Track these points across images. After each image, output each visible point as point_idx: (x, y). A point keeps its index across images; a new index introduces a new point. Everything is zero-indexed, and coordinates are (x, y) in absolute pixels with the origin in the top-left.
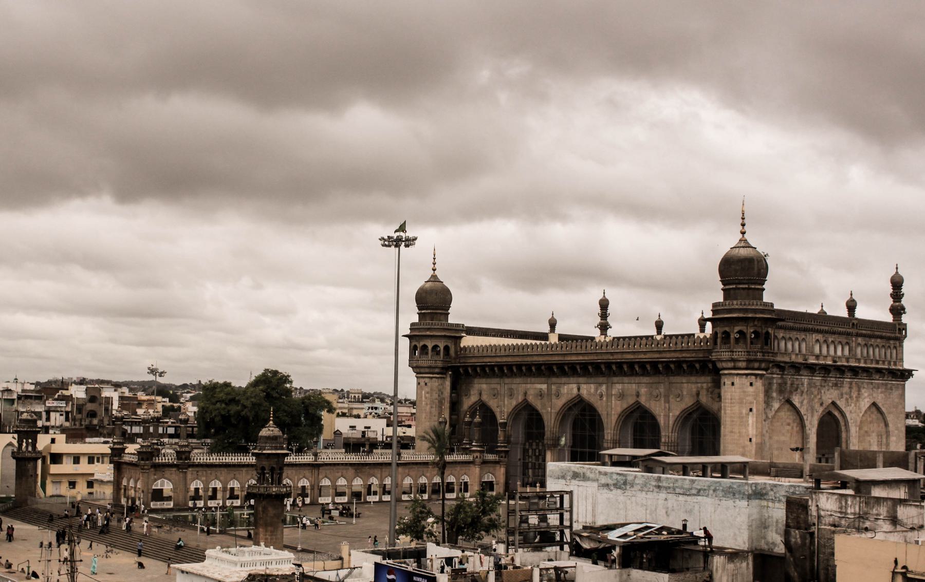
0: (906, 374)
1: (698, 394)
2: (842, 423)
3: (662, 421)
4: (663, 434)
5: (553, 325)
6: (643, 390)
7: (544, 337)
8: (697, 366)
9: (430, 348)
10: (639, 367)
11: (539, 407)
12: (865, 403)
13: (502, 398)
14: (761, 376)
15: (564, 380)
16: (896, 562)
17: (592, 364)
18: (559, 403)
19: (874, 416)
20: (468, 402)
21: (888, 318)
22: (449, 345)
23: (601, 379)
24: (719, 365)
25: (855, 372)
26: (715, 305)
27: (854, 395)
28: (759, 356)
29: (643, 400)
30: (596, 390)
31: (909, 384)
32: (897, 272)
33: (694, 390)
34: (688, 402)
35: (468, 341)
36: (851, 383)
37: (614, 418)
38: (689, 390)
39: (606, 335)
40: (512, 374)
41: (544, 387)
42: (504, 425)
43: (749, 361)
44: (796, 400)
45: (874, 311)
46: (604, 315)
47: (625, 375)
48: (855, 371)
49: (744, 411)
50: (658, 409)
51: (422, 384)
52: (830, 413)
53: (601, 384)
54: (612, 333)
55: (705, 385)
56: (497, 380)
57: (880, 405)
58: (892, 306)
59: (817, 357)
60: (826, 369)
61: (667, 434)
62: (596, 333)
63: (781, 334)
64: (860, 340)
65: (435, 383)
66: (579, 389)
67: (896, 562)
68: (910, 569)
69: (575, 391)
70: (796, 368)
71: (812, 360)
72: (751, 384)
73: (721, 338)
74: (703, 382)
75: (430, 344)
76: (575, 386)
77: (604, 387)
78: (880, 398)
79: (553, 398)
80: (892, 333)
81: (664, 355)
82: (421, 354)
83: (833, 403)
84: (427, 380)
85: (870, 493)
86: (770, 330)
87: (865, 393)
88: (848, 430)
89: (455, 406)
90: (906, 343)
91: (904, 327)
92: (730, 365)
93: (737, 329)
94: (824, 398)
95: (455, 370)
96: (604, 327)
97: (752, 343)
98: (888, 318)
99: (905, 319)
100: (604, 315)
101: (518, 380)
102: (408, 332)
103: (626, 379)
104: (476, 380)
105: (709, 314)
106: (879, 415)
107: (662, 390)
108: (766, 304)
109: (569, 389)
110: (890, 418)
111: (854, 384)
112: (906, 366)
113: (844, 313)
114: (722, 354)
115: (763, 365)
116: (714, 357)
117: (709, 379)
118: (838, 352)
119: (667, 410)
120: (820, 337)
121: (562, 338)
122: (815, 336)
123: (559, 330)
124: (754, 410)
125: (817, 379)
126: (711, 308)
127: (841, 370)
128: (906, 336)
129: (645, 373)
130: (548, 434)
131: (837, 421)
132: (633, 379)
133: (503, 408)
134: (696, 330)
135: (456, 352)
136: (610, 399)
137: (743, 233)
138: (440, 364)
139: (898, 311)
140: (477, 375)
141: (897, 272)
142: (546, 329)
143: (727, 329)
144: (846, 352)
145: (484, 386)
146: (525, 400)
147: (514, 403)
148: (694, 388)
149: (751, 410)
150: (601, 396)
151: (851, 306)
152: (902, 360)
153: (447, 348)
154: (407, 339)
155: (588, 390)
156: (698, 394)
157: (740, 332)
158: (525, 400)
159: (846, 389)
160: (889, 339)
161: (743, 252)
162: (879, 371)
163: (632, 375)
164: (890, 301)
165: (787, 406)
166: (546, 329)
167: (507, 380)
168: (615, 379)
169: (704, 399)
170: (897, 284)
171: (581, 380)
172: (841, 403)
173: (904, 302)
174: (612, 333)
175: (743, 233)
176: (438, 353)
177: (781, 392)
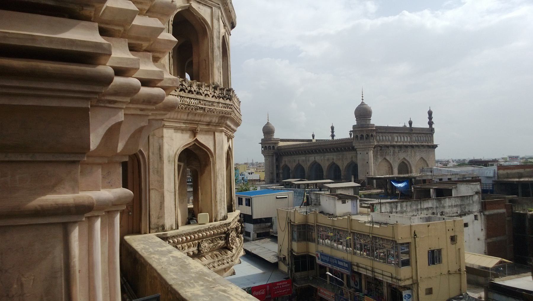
0: (435, 146)
4: (342, 172)
5: (313, 136)
6: (335, 158)
7: (311, 140)
12: (418, 158)
18: (309, 164)
24: (356, 147)
26: (354, 126)
29: (335, 161)
31: (436, 149)
34: (349, 161)
35: (281, 144)
37: (326, 168)
38: (348, 156)
40: (294, 154)
44: (388, 158)
45: (421, 123)
46: (333, 132)
47: (328, 152)
48: (412, 146)
50: (339, 164)
52: (403, 162)
54: (335, 138)
57: (424, 158)
59: (396, 142)
60: (400, 147)
62: (330, 138)
63: (381, 135)
64: (414, 135)
70: (387, 146)
71: (395, 143)
74: (352, 154)
75: (267, 146)
80: (430, 132)
82: (264, 149)
85: (336, 192)
87: (418, 154)
88: (411, 168)
89: (278, 167)
90: (435, 135)
95: (276, 154)
96: (333, 136)
97: (366, 139)
98: (428, 126)
99: (433, 126)
100: (333, 132)
103: (329, 154)
105: (352, 130)
108: (371, 125)
109: (312, 158)
110: (428, 162)
112: (435, 143)
113: (408, 126)
114: (356, 145)
118: (406, 140)
119: (343, 165)
120: (397, 135)
121: (316, 140)
122: (395, 135)
123: (316, 138)
125: (397, 150)
127: (406, 146)
129: (335, 152)
130: (306, 175)
131: (406, 165)
132: (331, 154)
133: (292, 166)
137: (363, 100)
139: (431, 123)
142: (312, 138)
146: (299, 163)
147: (295, 164)
151: (410, 123)
152: (433, 141)
153: (273, 147)
158: (299, 163)
159: (409, 153)
160: (428, 134)
162: (423, 146)
164: (428, 120)
165: (385, 160)
166: (312, 138)
167: (293, 157)
168: (326, 154)
169: (354, 159)
170: (430, 113)
172: (407, 158)
173: (433, 120)
174: (335, 138)
175: (363, 100)
177: (381, 155)
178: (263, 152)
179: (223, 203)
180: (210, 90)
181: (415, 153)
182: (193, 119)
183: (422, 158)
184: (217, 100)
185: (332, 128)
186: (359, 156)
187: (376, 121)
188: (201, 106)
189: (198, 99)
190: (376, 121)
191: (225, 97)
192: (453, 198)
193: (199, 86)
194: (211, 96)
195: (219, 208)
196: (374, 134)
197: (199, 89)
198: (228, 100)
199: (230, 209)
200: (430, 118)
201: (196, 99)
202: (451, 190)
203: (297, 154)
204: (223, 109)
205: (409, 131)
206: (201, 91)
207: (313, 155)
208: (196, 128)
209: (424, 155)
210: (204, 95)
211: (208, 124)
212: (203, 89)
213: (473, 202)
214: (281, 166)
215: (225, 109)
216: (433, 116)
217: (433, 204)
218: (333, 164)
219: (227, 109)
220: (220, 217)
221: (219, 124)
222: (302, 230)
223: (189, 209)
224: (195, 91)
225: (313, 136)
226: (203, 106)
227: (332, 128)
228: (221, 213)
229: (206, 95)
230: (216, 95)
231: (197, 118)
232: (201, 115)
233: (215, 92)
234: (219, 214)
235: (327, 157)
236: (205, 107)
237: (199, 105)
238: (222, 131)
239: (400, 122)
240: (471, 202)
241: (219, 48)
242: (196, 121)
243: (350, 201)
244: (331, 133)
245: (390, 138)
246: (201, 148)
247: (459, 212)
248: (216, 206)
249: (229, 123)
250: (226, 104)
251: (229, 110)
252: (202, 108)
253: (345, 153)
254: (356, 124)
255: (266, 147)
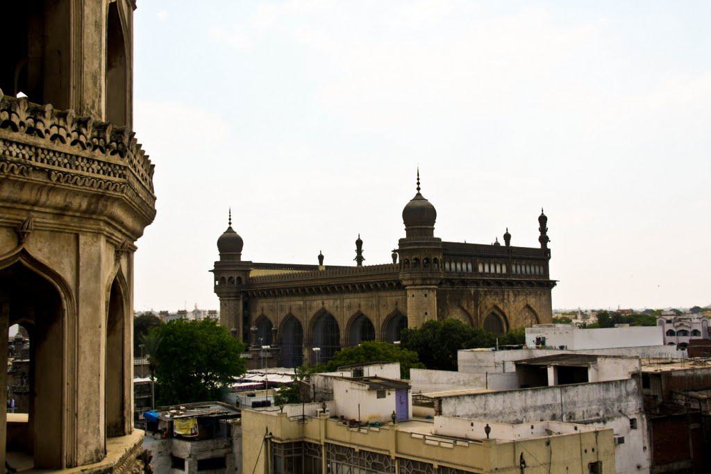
0: (554, 283)
1: (397, 303)
2: (502, 318)
3: (375, 323)
4: (376, 332)
5: (321, 258)
6: (363, 303)
8: (394, 284)
9: (227, 280)
10: (359, 286)
11: (299, 318)
13: (274, 311)
14: (433, 289)
15: (314, 297)
16: (267, 429)
17: (329, 285)
18: (311, 314)
19: (527, 314)
20: (256, 315)
21: (538, 245)
22: (241, 276)
23: (336, 296)
24: (404, 283)
25: (510, 284)
27: (512, 299)
28: (430, 275)
29: (363, 310)
30: (334, 303)
31: (554, 291)
32: (543, 214)
33: (394, 301)
34: (391, 310)
35: (254, 273)
36: (509, 292)
37: (346, 323)
39: (361, 264)
40: (281, 295)
41: (301, 303)
42: (276, 331)
43: (424, 279)
45: (526, 239)
46: (359, 251)
48: (510, 284)
49: (422, 314)
51: (223, 305)
52: (493, 313)
53: (336, 299)
54: (364, 264)
55: (400, 297)
56: (271, 300)
57: (532, 306)
58: (540, 237)
61: (377, 333)
62: (355, 264)
65: (232, 304)
66: (323, 304)
67: (267, 429)
68: (273, 435)
69: (321, 305)
72: (426, 295)
73: (404, 263)
75: (227, 276)
76: (320, 302)
77: (338, 302)
78: (532, 301)
79: (307, 309)
80: (541, 256)
81: (374, 277)
83: (496, 307)
84: (226, 302)
86: (437, 257)
89: (247, 320)
90: (551, 262)
91: (549, 251)
92: (410, 282)
93: (414, 257)
94: (488, 303)
95: (246, 294)
96: (360, 259)
98: (538, 245)
99: (549, 245)
100: (359, 251)
101: (285, 299)
102: (213, 268)
103: (352, 296)
104: (259, 301)
105: (397, 248)
106: (532, 314)
107: (374, 302)
109: (317, 303)
111: (511, 293)
112: (552, 278)
113: (503, 243)
114: (404, 277)
115: (434, 282)
116: (401, 277)
117: (403, 292)
123: (325, 263)
124: (429, 314)
126: (398, 243)
127: (499, 283)
128: (550, 257)
129: (363, 291)
130: (305, 336)
131: (499, 319)
132: (356, 295)
133: (277, 319)
134: (390, 261)
135: (246, 281)
136: (342, 308)
137: (419, 189)
138: (235, 290)
139: (544, 239)
140: (260, 297)
141: (543, 214)
142: (317, 263)
143: (407, 257)
144: (504, 270)
145: (265, 304)
146: (290, 313)
148: (394, 299)
149: (426, 314)
150: (337, 307)
151: (507, 237)
153: (239, 279)
154: (212, 274)
155: (330, 303)
156: (397, 303)
157: (416, 259)
158: (290, 313)
161: (418, 203)
163: (355, 292)
164: (539, 234)
166: (317, 263)
167: (279, 299)
168: (345, 296)
169: (400, 307)
170: (543, 220)
171: (325, 297)
174: (364, 264)
176: (233, 283)
178: (217, 290)
179: (93, 417)
180: (69, 127)
181: (515, 296)
182: (15, 196)
183: (528, 307)
184: (87, 153)
185: (359, 243)
186: (410, 302)
187: (446, 230)
188: (39, 164)
189: (30, 147)
190: (446, 230)
191: (108, 146)
192: (590, 386)
193: (36, 114)
194: (69, 141)
195: (81, 431)
196: (440, 257)
197: (36, 121)
198: (117, 156)
199: (116, 430)
200: (543, 229)
201: (24, 145)
202: (585, 371)
203: (287, 295)
204: (101, 176)
205: (503, 253)
206: (40, 126)
207: (319, 297)
208: (24, 222)
209: (532, 301)
210: (48, 137)
211: (61, 212)
212: (48, 123)
213: (628, 394)
214: (254, 320)
215: (106, 177)
216: (548, 225)
217: (554, 398)
218: (359, 315)
219: (112, 178)
220: (82, 455)
221: (89, 214)
222: (294, 455)
223: (12, 426)
224: (22, 124)
225: (321, 258)
226: (44, 165)
227: (359, 243)
228: (86, 445)
229: (54, 138)
230: (82, 138)
231: (26, 195)
232: (41, 188)
233: (80, 133)
234: (81, 446)
235: (347, 301)
236: (50, 167)
237: (33, 162)
238: (97, 233)
239: (486, 236)
240: (624, 393)
241: (97, 25)
242: (26, 203)
243: (393, 394)
244: (356, 254)
245: (470, 266)
246: (37, 275)
247: (601, 413)
248: (74, 427)
249: (118, 212)
250: (110, 164)
251: (117, 179)
252: (42, 170)
253: (382, 294)
254: (404, 236)
255: (223, 279)
